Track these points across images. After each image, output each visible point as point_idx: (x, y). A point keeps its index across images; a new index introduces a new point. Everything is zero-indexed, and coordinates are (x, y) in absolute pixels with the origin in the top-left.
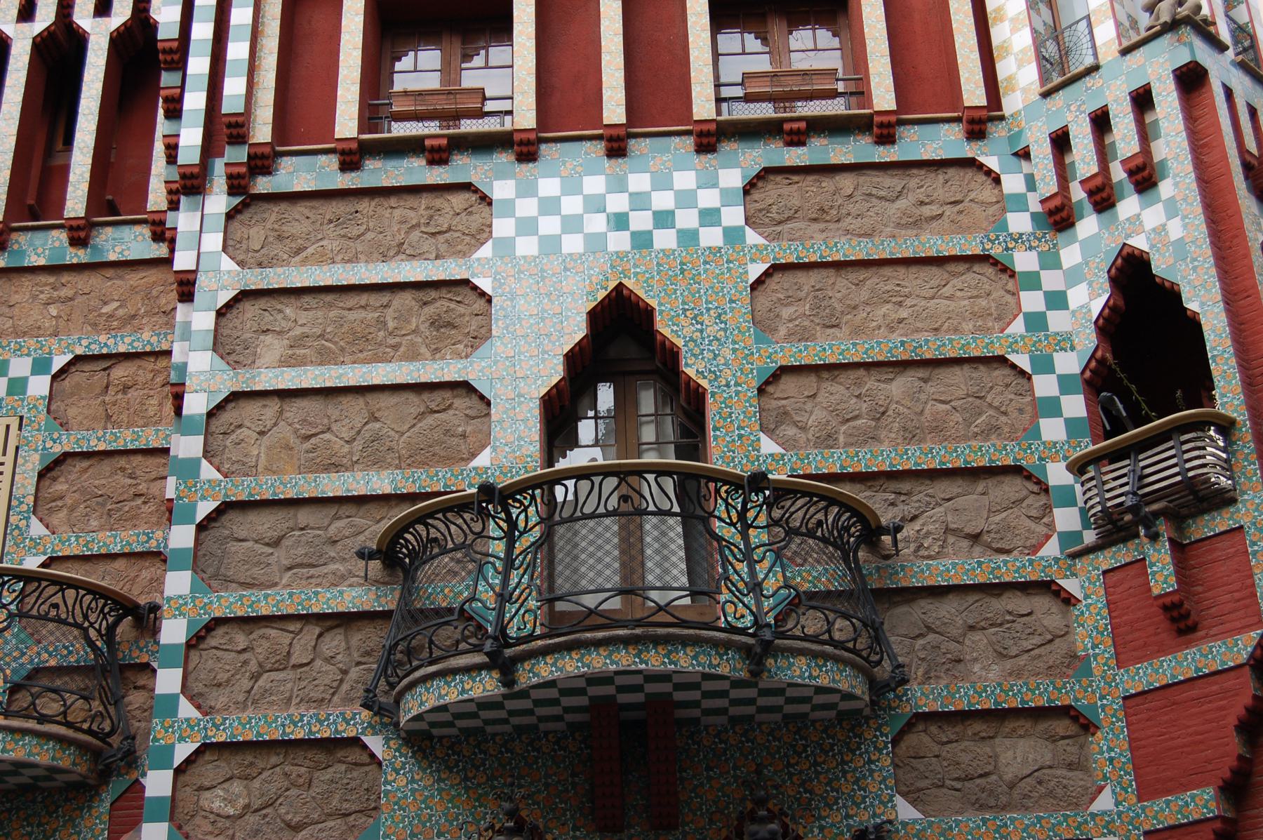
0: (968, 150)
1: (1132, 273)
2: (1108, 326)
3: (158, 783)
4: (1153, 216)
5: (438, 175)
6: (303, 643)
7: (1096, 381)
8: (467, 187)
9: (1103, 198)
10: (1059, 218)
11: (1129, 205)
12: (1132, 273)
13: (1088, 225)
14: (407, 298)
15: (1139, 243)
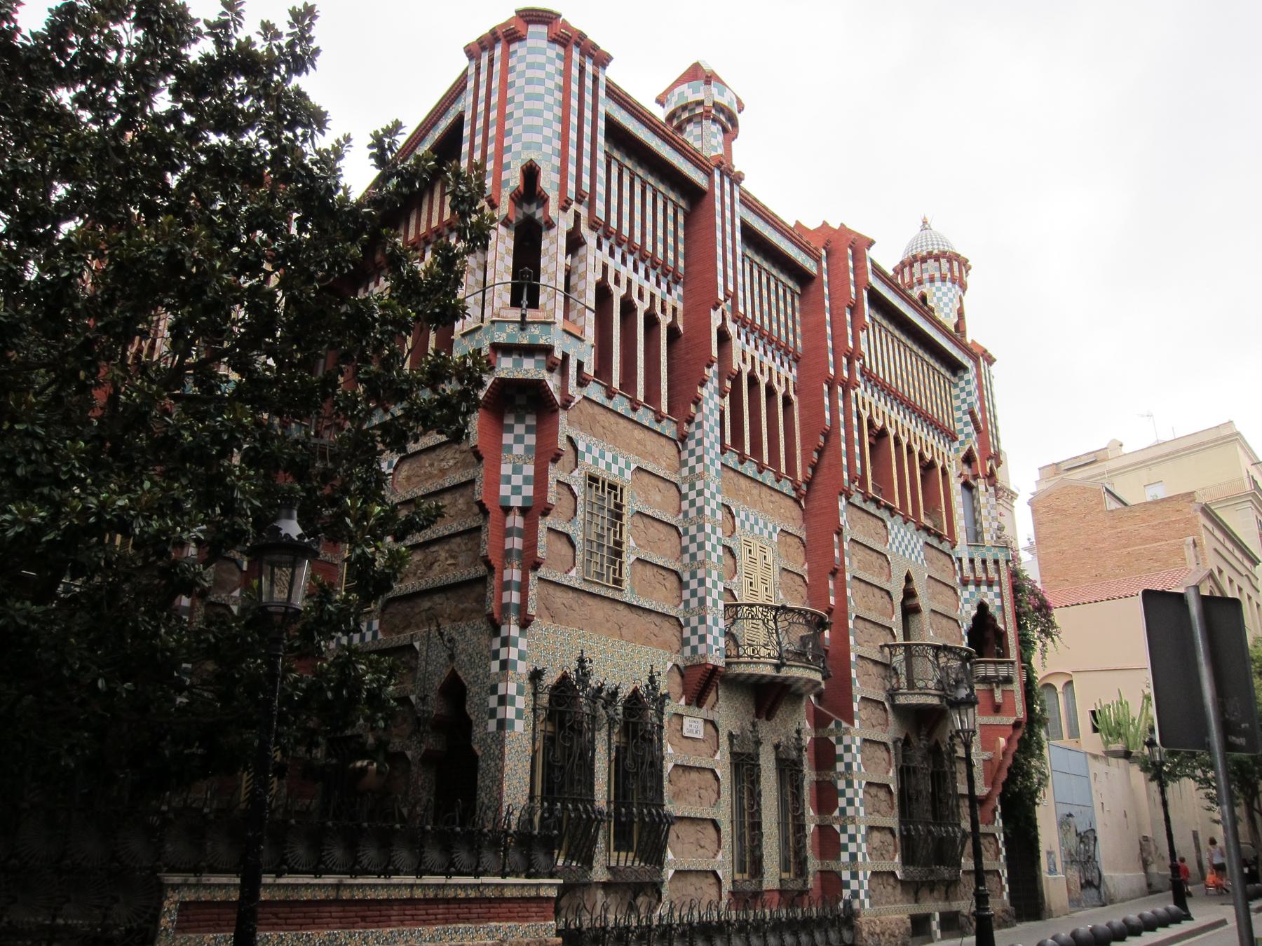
0: (951, 552)
1: (982, 607)
2: (974, 619)
3: (856, 707)
4: (991, 595)
5: (878, 513)
6: (870, 666)
7: (970, 634)
8: (882, 520)
9: (978, 583)
10: (965, 583)
11: (984, 588)
12: (982, 607)
13: (972, 588)
14: (875, 555)
15: (986, 601)
